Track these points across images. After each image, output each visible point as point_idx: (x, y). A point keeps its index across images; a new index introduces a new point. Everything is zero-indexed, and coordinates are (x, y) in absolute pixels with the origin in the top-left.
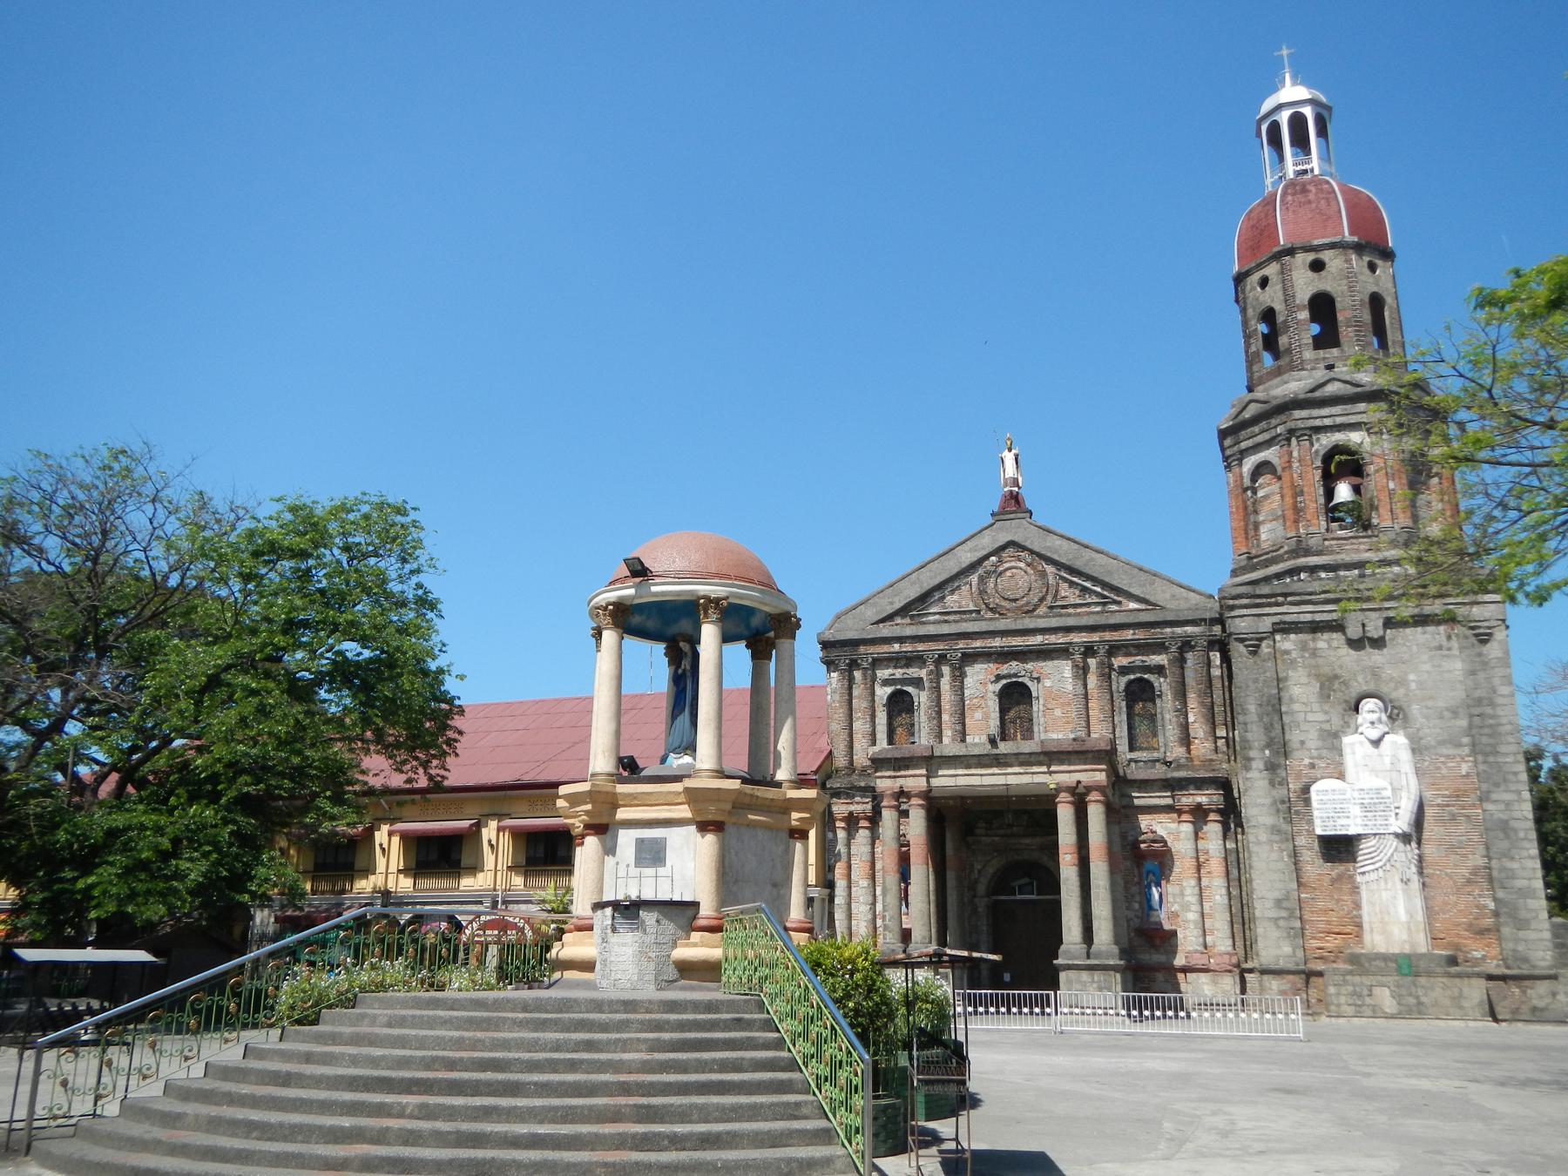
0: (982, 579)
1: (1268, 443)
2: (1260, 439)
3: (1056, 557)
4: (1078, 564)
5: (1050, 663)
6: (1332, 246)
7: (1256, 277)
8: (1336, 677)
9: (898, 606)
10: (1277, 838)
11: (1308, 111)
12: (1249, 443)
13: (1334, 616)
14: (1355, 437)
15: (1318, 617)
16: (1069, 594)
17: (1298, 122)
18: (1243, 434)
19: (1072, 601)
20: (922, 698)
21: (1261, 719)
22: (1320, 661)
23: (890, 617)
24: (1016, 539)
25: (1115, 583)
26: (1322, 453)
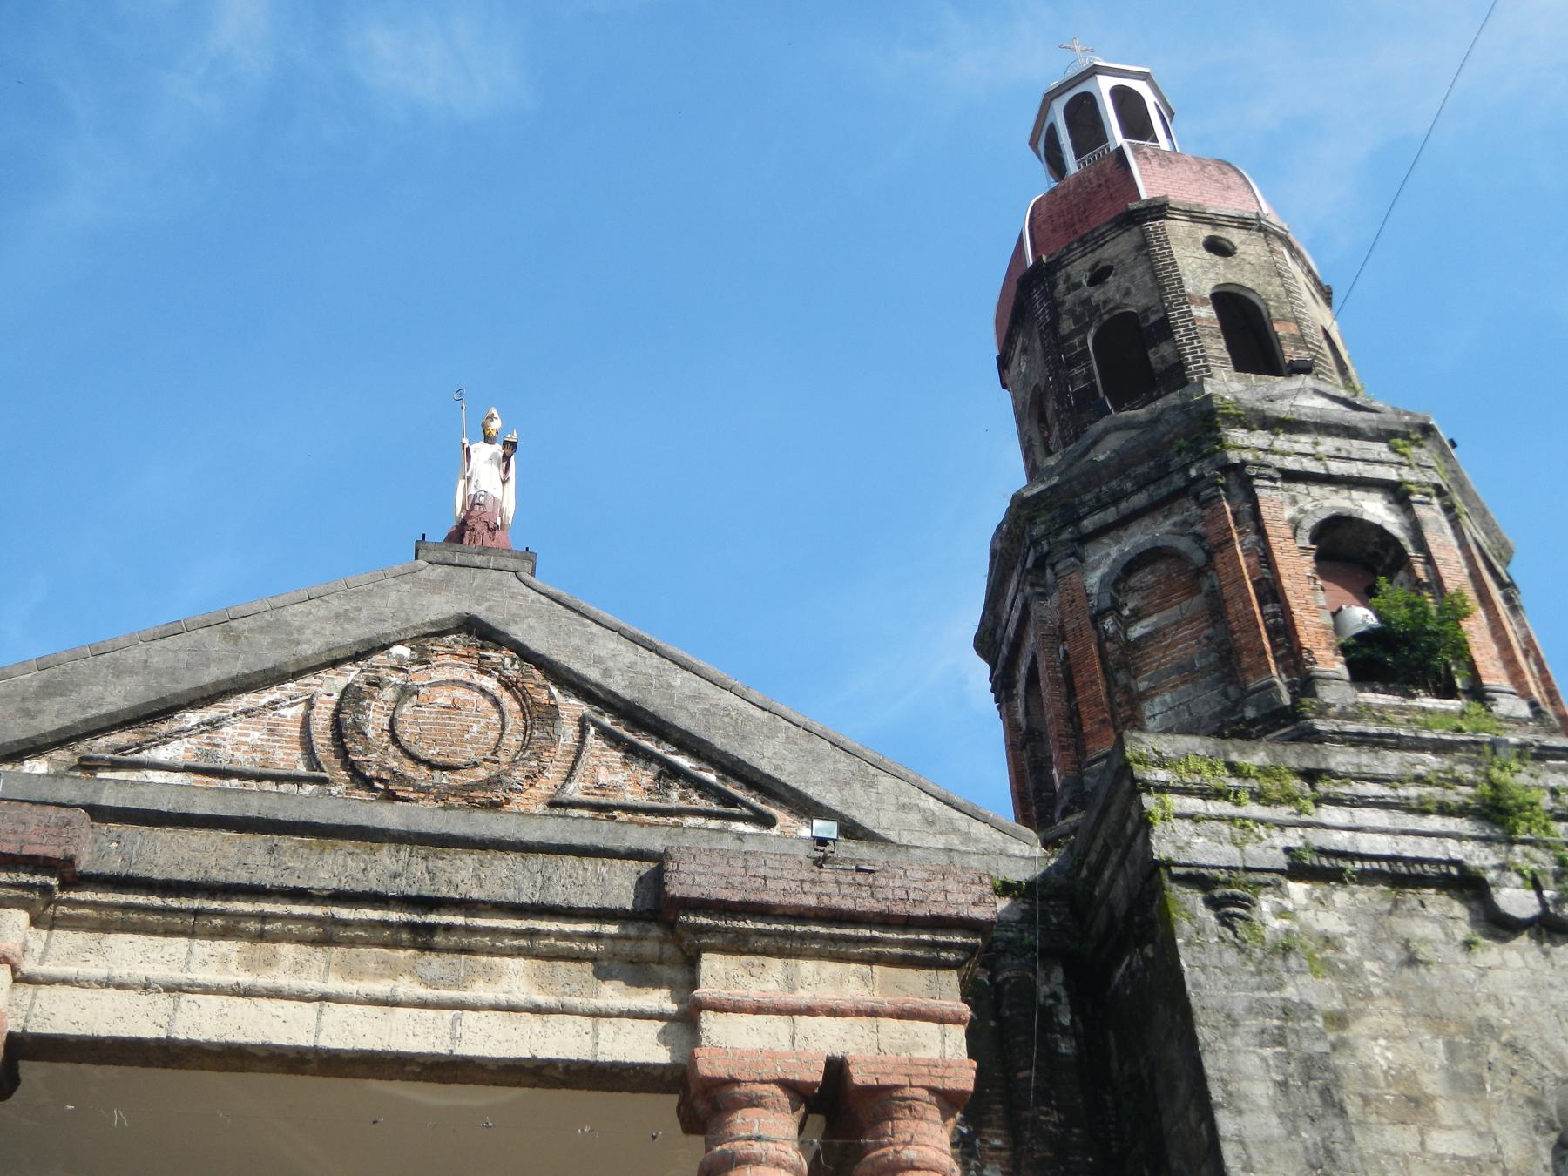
3: (593, 674)
4: (655, 703)
6: (1245, 223)
8: (1486, 1027)
9: (51, 718)
11: (1141, 87)
14: (1375, 509)
15: (1409, 847)
16: (629, 782)
17: (1127, 101)
19: (632, 796)
21: (1294, 1131)
22: (1434, 977)
24: (480, 611)
25: (767, 768)
26: (1309, 523)
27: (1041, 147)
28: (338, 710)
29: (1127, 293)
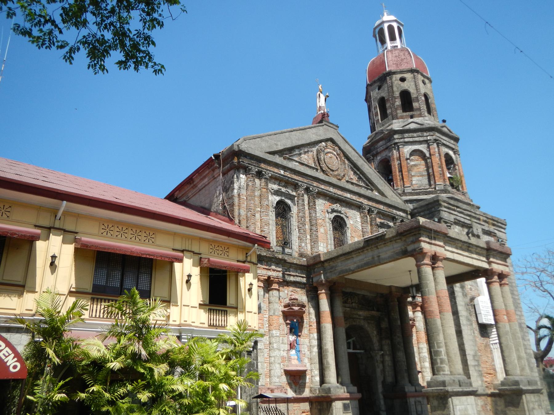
0: (318, 152)
1: (420, 142)
2: (417, 139)
3: (350, 155)
5: (351, 211)
7: (399, 76)
9: (280, 148)
10: (468, 323)
12: (411, 140)
13: (469, 222)
14: (451, 153)
16: (355, 179)
18: (406, 135)
19: (354, 181)
20: (294, 209)
23: (273, 153)
25: (372, 179)
27: (377, 30)
28: (317, 155)
29: (409, 87)
